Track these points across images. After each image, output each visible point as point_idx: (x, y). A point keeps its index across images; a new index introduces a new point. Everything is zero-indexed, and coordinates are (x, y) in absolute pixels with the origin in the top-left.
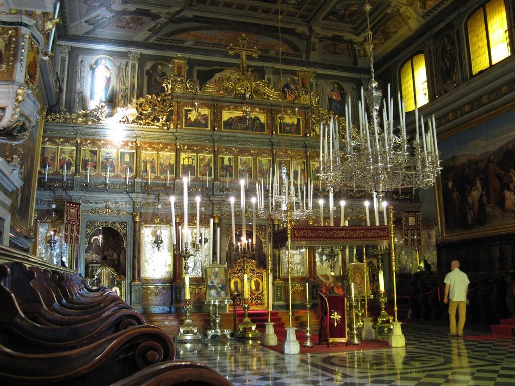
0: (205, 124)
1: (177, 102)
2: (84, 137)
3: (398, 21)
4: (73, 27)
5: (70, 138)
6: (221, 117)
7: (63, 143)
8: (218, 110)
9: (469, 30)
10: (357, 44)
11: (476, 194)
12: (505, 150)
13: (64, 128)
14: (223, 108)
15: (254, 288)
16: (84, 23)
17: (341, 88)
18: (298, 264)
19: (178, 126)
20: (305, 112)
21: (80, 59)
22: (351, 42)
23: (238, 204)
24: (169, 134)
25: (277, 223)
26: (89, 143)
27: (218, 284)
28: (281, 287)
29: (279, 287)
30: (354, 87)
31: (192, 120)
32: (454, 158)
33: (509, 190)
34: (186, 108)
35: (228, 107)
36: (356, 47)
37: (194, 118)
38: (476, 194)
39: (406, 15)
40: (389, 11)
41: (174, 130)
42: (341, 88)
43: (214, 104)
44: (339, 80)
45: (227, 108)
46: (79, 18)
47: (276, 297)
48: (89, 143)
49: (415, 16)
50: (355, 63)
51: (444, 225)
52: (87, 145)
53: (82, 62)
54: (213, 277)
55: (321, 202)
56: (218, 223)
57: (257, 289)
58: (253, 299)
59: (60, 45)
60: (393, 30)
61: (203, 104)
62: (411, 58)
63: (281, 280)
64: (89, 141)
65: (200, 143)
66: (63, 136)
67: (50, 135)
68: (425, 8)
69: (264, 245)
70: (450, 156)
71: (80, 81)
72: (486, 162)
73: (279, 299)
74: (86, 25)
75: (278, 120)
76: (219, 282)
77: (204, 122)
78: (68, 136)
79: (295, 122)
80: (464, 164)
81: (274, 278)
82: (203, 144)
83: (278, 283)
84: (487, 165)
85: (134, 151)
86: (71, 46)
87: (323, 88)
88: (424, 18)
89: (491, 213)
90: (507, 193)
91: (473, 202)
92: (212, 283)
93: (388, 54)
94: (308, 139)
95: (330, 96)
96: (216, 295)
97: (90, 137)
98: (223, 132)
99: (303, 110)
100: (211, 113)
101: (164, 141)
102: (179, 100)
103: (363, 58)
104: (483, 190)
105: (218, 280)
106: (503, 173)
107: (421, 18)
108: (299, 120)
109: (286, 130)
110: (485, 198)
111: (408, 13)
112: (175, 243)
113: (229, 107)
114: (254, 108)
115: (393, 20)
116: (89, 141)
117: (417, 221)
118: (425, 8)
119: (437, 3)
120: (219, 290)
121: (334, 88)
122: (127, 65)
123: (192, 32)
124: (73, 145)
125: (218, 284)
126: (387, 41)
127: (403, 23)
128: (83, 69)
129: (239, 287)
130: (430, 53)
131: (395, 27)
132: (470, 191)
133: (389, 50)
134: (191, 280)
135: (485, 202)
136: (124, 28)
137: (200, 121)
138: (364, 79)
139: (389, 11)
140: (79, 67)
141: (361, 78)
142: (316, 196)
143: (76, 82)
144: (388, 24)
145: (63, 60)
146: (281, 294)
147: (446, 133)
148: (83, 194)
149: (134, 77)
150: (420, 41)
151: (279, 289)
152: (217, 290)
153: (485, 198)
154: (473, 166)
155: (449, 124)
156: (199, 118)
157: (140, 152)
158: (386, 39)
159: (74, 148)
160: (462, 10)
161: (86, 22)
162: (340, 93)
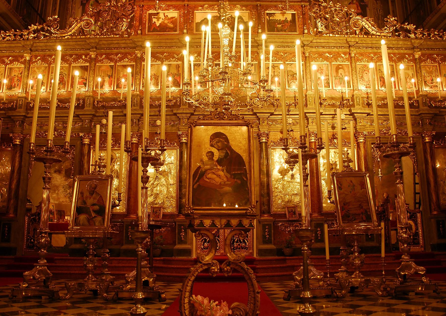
0: (173, 28)
2: (34, 53)
5: (19, 56)
6: (193, 18)
7: (11, 62)
8: (189, 12)
14: (196, 8)
18: (296, 194)
19: (139, 32)
20: (302, 6)
24: (128, 41)
25: (264, 141)
27: (94, 205)
29: (267, 225)
31: (158, 24)
34: (151, 11)
35: (201, 6)
37: (160, 22)
43: (185, 5)
45: (200, 8)
47: (265, 241)
61: (172, 5)
63: (271, 216)
64: (39, 58)
65: (166, 50)
66: (12, 54)
73: (265, 241)
77: (171, 25)
78: (16, 54)
79: (289, 18)
82: (170, 50)
83: (266, 220)
92: (85, 203)
96: (86, 223)
98: (196, 34)
100: (180, 15)
101: (123, 51)
105: (94, 199)
108: (293, 15)
109: (277, 28)
113: (202, 6)
114: (236, 5)
116: (39, 58)
120: (93, 215)
124: (22, 63)
125: (94, 205)
137: (166, 25)
146: (270, 235)
151: (267, 227)
152: (90, 215)
156: (166, 22)
157: (95, 64)
159: (23, 66)
162: (361, 6)
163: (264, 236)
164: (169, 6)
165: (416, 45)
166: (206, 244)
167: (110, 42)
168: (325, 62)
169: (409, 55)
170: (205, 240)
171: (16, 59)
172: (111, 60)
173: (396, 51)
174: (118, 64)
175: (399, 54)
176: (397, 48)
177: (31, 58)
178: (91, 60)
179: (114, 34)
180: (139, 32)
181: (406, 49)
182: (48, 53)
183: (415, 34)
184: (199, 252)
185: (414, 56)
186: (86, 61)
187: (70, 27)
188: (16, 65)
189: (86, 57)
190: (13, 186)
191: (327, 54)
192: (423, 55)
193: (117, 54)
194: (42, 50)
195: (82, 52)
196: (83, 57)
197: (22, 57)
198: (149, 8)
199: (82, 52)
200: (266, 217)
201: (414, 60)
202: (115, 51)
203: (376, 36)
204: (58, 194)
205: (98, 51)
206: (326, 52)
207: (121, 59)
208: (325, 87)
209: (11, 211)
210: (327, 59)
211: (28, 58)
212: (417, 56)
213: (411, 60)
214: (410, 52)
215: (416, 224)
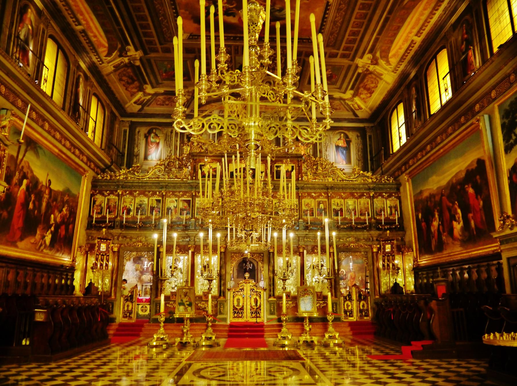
1: (194, 159)
2: (124, 189)
3: (372, 78)
4: (128, 107)
7: (109, 195)
9: (428, 79)
10: (348, 99)
11: (436, 223)
12: (451, 183)
13: (110, 184)
15: (253, 304)
16: (134, 104)
17: (346, 136)
19: (194, 178)
21: (137, 130)
22: (341, 99)
23: (206, 238)
26: (128, 194)
28: (274, 303)
30: (359, 135)
32: (421, 192)
33: (456, 221)
36: (350, 103)
38: (436, 223)
39: (378, 73)
40: (360, 71)
41: (191, 181)
42: (346, 136)
44: (345, 130)
46: (128, 101)
48: (128, 194)
49: (386, 72)
50: (355, 115)
51: (418, 252)
52: (126, 195)
53: (139, 132)
54: (183, 296)
55: (276, 234)
56: (224, 252)
57: (256, 305)
58: (252, 313)
59: (123, 121)
60: (373, 85)
61: (214, 160)
62: (396, 107)
63: (275, 298)
67: (100, 189)
68: (390, 64)
69: (262, 269)
70: (418, 191)
71: (137, 146)
72: (440, 196)
73: (271, 313)
74: (135, 105)
75: (275, 168)
76: (187, 300)
80: (427, 197)
81: (270, 296)
83: (272, 301)
84: (441, 198)
85: (160, 198)
86: (131, 121)
87: (330, 138)
88: (395, 73)
89: (446, 241)
90: (455, 223)
91: (434, 231)
92: (182, 300)
93: (380, 105)
94: (300, 182)
95: (337, 144)
97: (129, 189)
99: (297, 159)
101: (183, 190)
102: (195, 158)
103: (360, 110)
104: (439, 221)
106: (451, 205)
107: (393, 73)
110: (441, 227)
111: (377, 71)
112: (155, 269)
115: (367, 77)
117: (392, 248)
118: (390, 64)
119: (398, 59)
120: (187, 306)
121: (341, 137)
122: (172, 132)
123: (213, 104)
124: (116, 195)
126: (373, 95)
127: (377, 79)
128: (139, 137)
129: (241, 304)
130: (406, 101)
131: (372, 83)
132: (432, 222)
133: (379, 102)
134: (212, 297)
135: (441, 231)
136: (163, 105)
138: (368, 127)
139: (360, 71)
140: (136, 137)
141: (365, 127)
142: (273, 229)
143: (134, 148)
144: (365, 80)
145: (125, 131)
146: (274, 310)
147: (415, 171)
148: (121, 232)
149: (177, 141)
150: (400, 92)
153: (441, 227)
154: (433, 199)
155: (419, 162)
158: (371, 93)
159: (117, 198)
160: (422, 62)
161: (135, 103)
163: (271, 310)
164: (213, 160)
165: (371, 187)
166: (236, 315)
167: (175, 184)
168: (312, 199)
169: (367, 193)
170: (235, 312)
171: (112, 192)
172: (176, 196)
173: (358, 191)
174: (180, 199)
175: (360, 193)
176: (359, 189)
177: (122, 193)
178: (163, 196)
179: (177, 178)
180: (194, 178)
181: (365, 189)
182: (134, 189)
183: (371, 178)
184: (231, 319)
185: (369, 194)
186: (159, 196)
187: (148, 172)
188: (112, 197)
189: (159, 193)
190: (114, 279)
191: (313, 194)
192: (375, 193)
193: (179, 192)
194: (129, 188)
195: (157, 190)
196: (158, 193)
197: (116, 191)
198: (200, 161)
199: (157, 190)
200: (272, 299)
201: (369, 197)
202: (178, 190)
203: (346, 180)
204: (128, 276)
205: (167, 190)
206: (312, 193)
207: (183, 196)
208: (310, 215)
209: (113, 295)
210: (312, 197)
211: (120, 193)
212: (371, 195)
213: (367, 197)
214: (368, 191)
215: (367, 304)
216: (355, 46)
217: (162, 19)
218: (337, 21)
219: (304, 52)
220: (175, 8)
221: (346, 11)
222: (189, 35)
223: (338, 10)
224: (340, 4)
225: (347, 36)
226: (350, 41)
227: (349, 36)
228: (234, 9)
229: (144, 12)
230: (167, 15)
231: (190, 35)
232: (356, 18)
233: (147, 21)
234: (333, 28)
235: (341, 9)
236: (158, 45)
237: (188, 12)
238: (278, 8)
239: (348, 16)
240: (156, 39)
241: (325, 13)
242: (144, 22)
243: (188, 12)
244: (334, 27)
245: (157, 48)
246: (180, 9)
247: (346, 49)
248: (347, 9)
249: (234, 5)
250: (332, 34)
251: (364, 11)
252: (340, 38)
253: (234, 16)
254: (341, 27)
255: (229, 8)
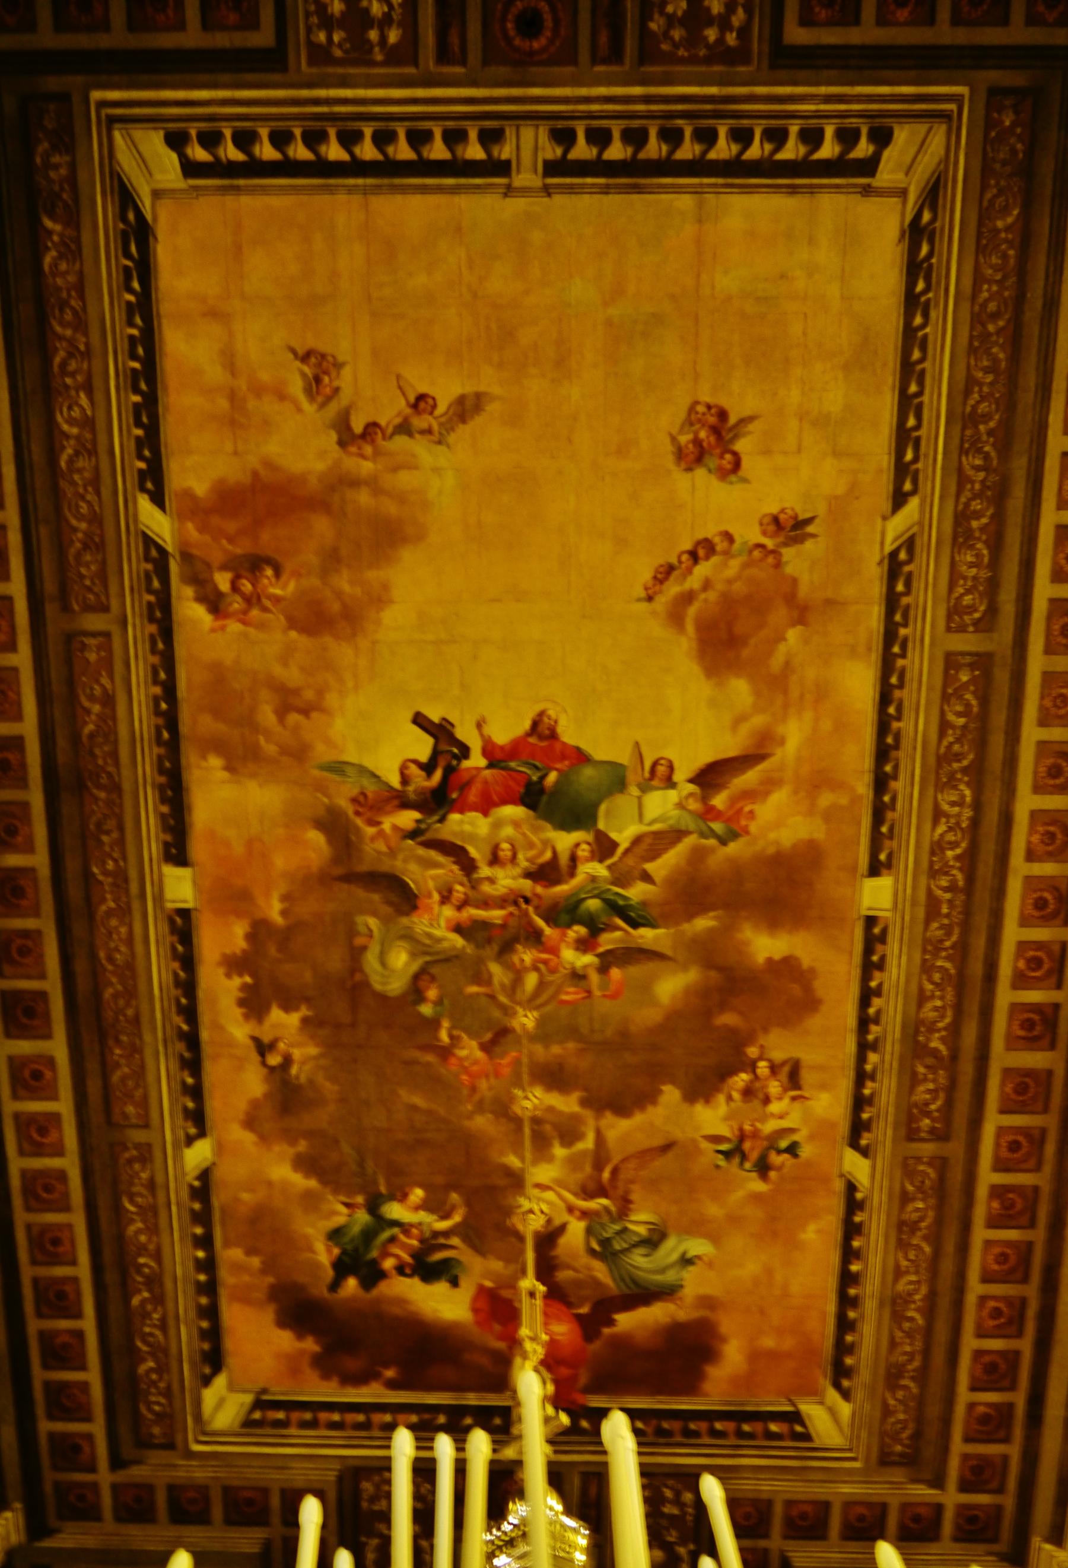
216: (1014, 1451)
217: (144, 1302)
218: (906, 1299)
219: (778, 1510)
220: (206, 1242)
221: (935, 1238)
222: (248, 1399)
223: (903, 1230)
224: (905, 1198)
225: (964, 1395)
226: (985, 1419)
227: (973, 1389)
228: (455, 1241)
229: (74, 1263)
230: (169, 1285)
231: (259, 1404)
232: (987, 1278)
233: (78, 1315)
234: (893, 1344)
235: (914, 1227)
236: (104, 1477)
237: (256, 1262)
238: (642, 1230)
239: (948, 1266)
240: (97, 1428)
241: (848, 1254)
242: (64, 1324)
243: (256, 1262)
244: (899, 1334)
245: (95, 1487)
246: (227, 1244)
247: (977, 1475)
248: (939, 1222)
249: (457, 1218)
250: (893, 1377)
251: (1012, 1235)
252: (933, 1411)
253: (455, 1283)
254: (928, 1332)
255: (436, 1234)
